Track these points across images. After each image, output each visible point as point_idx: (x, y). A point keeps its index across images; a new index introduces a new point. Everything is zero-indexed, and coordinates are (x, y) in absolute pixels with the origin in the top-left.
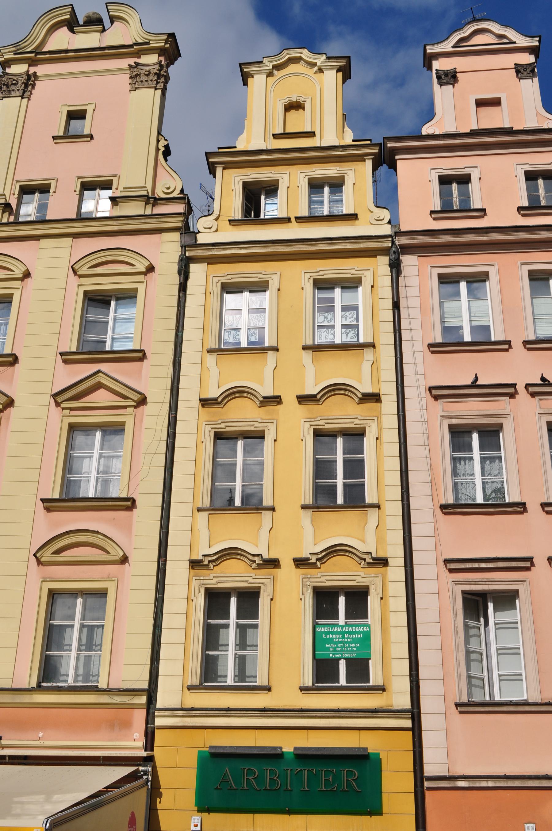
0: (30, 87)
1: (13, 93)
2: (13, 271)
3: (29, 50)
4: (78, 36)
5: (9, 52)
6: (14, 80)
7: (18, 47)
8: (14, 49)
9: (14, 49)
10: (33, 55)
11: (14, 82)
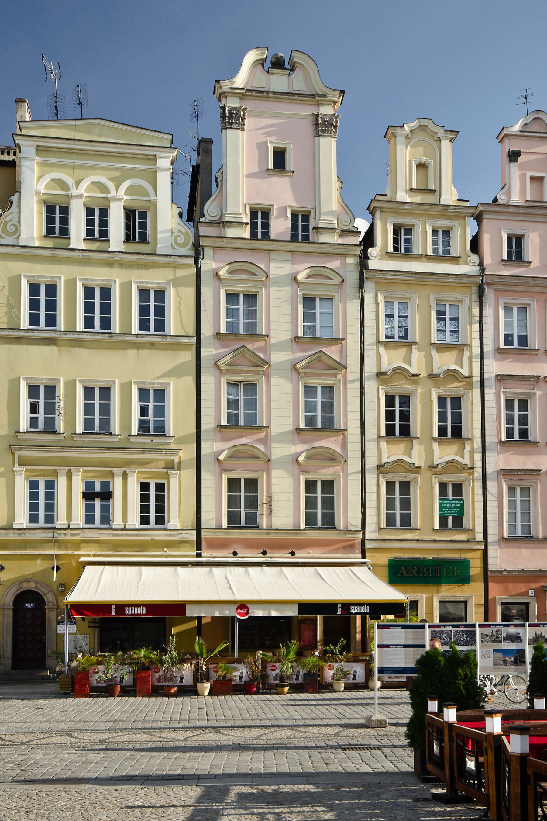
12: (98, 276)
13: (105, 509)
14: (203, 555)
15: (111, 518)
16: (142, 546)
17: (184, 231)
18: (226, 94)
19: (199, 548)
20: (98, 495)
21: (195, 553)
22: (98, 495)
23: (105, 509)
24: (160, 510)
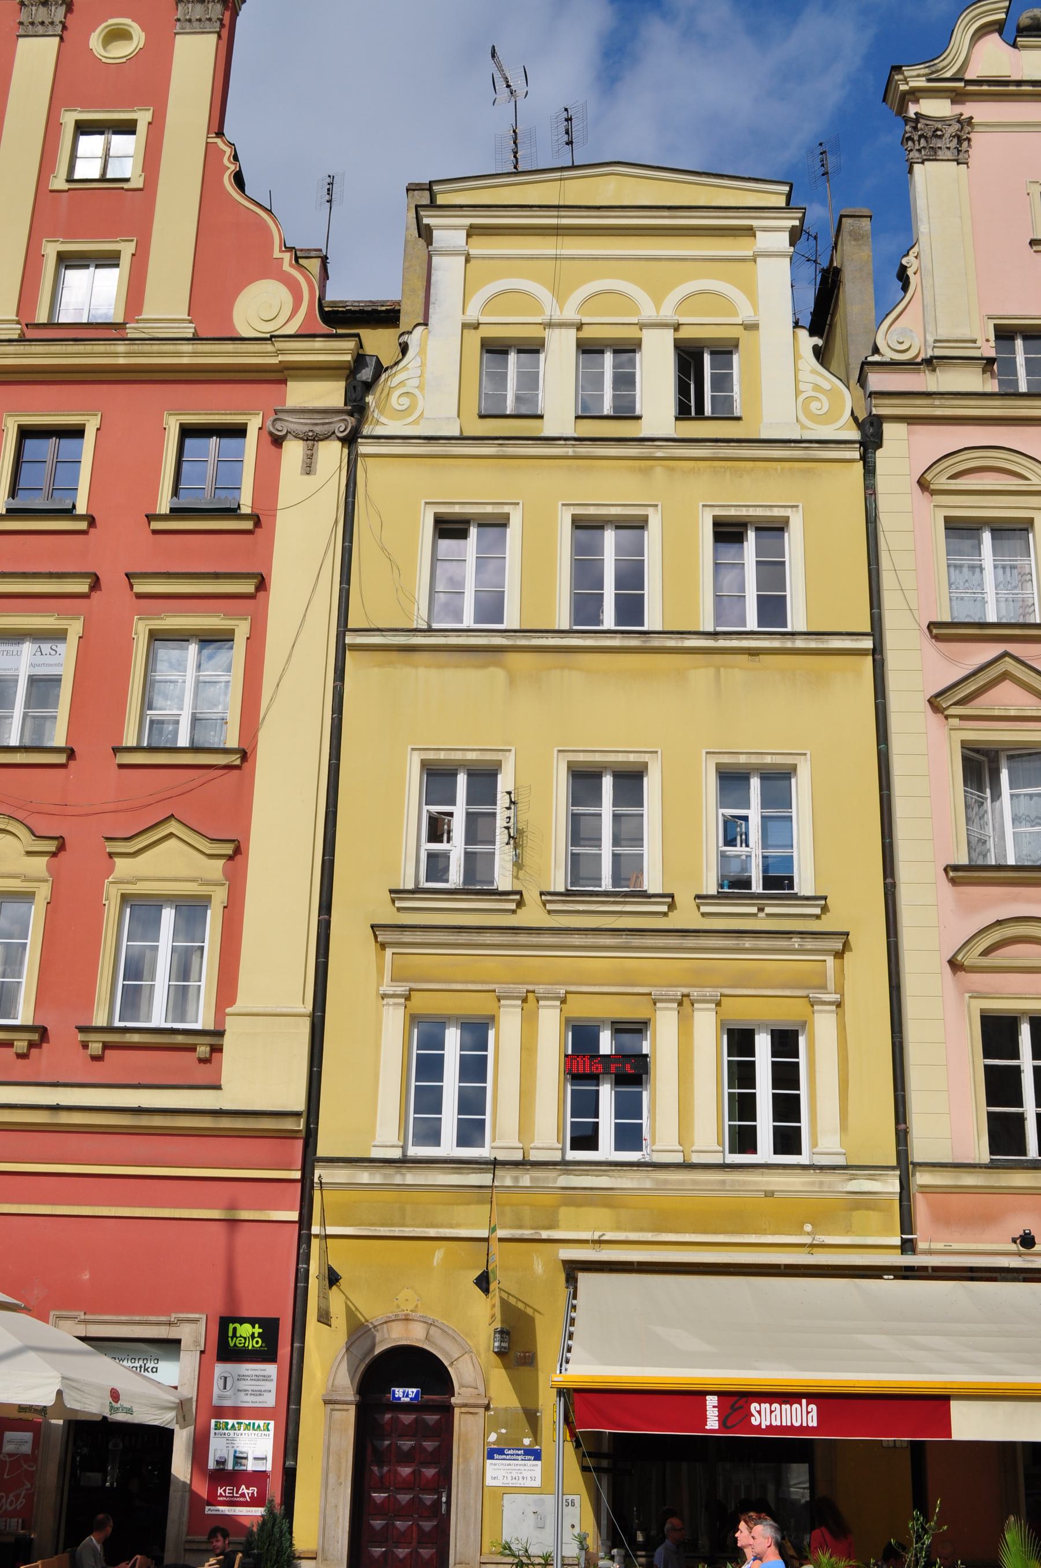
0: (965, 143)
1: (940, 152)
2: (1029, 479)
3: (948, 75)
4: (1025, 54)
5: (918, 76)
6: (937, 130)
7: (933, 69)
8: (927, 71)
9: (927, 71)
10: (962, 84)
11: (939, 133)
12: (610, 488)
13: (629, 1108)
14: (921, 1245)
15: (646, 1133)
16: (737, 1219)
17: (827, 386)
18: (919, 94)
19: (907, 1224)
20: (607, 1067)
21: (897, 1241)
22: (607, 1067)
23: (629, 1108)
24: (787, 1108)
